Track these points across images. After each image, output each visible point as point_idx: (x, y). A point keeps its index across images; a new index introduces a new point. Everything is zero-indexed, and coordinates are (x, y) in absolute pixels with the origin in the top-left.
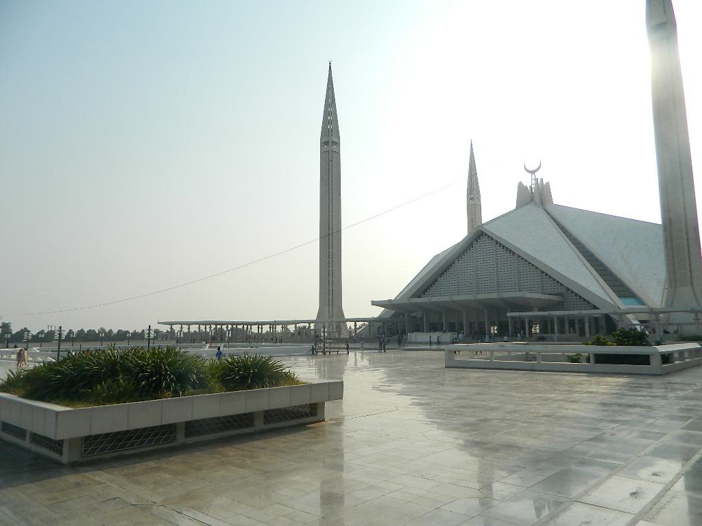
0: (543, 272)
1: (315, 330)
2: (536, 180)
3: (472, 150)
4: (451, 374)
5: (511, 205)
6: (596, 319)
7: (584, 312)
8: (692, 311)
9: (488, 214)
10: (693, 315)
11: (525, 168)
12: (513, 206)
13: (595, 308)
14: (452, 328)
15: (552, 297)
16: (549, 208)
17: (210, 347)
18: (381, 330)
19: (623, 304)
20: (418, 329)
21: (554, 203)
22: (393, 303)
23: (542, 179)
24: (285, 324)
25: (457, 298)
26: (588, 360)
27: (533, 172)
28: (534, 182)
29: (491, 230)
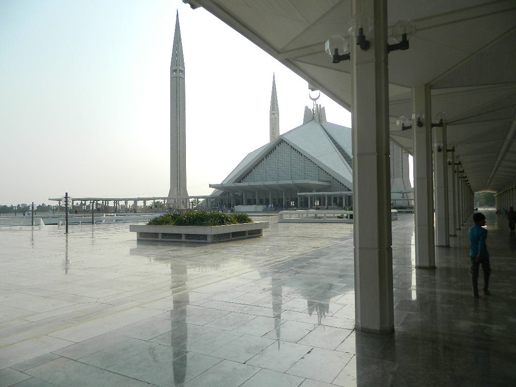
0: (319, 167)
1: (168, 204)
2: (317, 105)
4: (279, 224)
5: (300, 122)
7: (342, 193)
9: (284, 128)
11: (311, 98)
12: (301, 122)
13: (349, 190)
14: (261, 203)
15: (324, 183)
16: (323, 124)
18: (214, 204)
20: (238, 203)
21: (328, 120)
22: (224, 186)
23: (320, 105)
24: (145, 200)
25: (267, 183)
26: (347, 217)
27: (315, 100)
28: (315, 107)
29: (288, 138)
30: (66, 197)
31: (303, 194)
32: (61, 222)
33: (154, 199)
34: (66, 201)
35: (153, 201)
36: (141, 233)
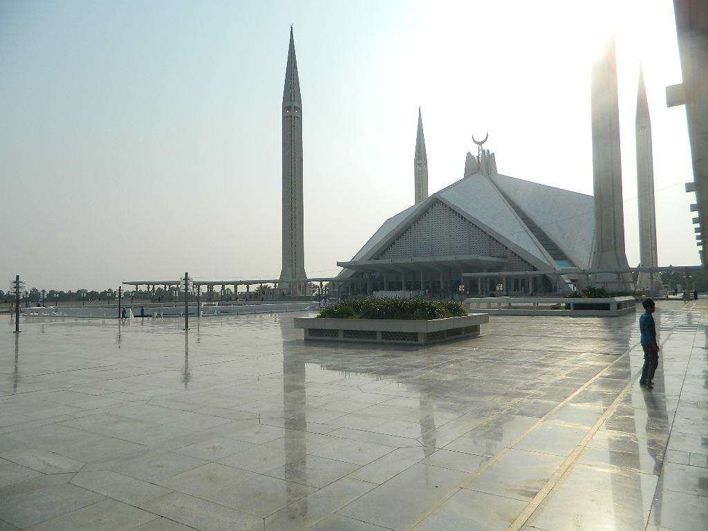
0: (490, 237)
2: (483, 151)
3: (420, 119)
5: (459, 174)
6: (535, 279)
8: (616, 272)
10: (615, 276)
13: (535, 269)
15: (499, 260)
17: (219, 305)
19: (558, 266)
21: (498, 172)
23: (488, 151)
24: (248, 283)
27: (480, 144)
28: (481, 152)
30: (186, 279)
31: (472, 274)
32: (156, 314)
33: (261, 282)
34: (186, 285)
35: (259, 285)
36: (310, 329)
